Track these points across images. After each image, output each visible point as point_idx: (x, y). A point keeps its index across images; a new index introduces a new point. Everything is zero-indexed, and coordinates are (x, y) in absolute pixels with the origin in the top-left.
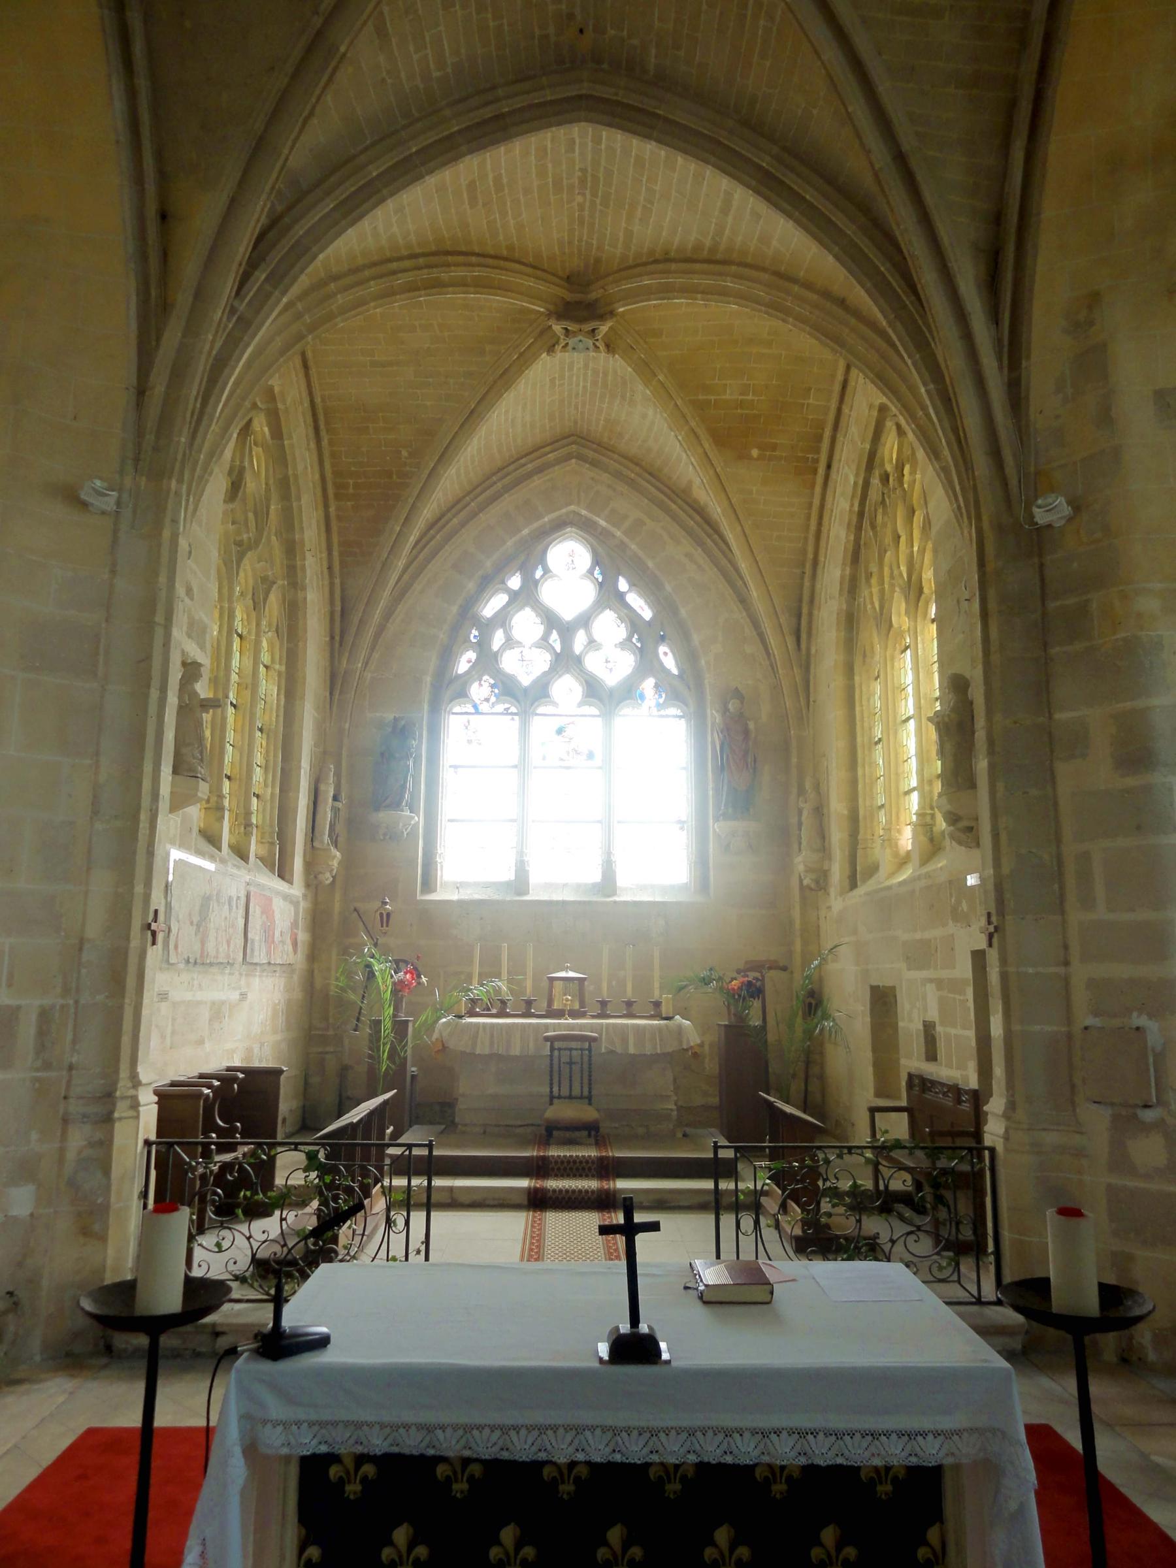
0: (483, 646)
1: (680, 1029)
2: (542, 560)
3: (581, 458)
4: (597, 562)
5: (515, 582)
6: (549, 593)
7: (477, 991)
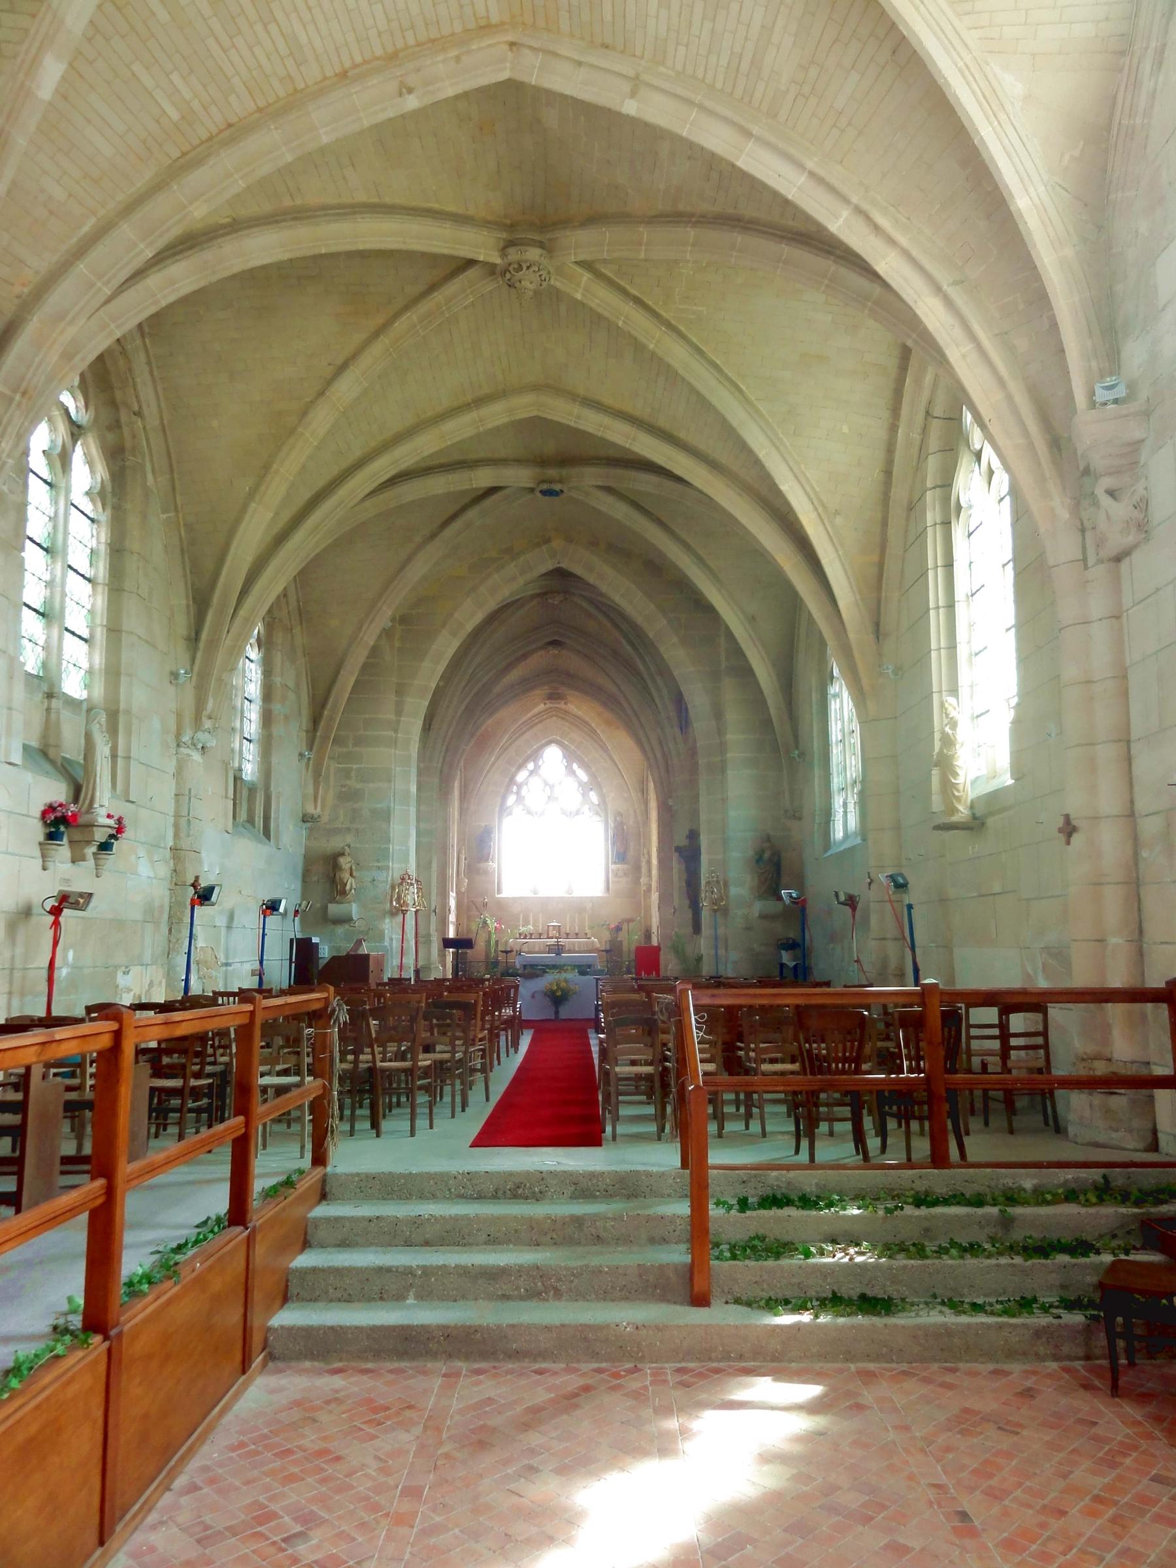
0: (518, 793)
1: (593, 942)
2: (542, 757)
3: (556, 716)
4: (565, 757)
5: (531, 766)
6: (543, 771)
7: (522, 929)
